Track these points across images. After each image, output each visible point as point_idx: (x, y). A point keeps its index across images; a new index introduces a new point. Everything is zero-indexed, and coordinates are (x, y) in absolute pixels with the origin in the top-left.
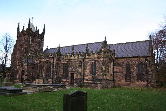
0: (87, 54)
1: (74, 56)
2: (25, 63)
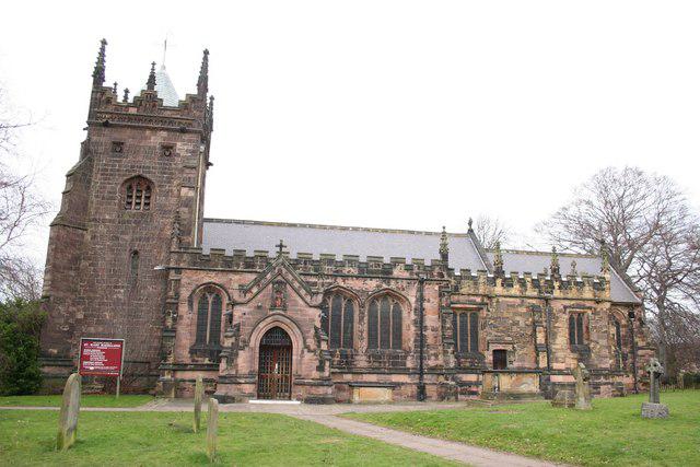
0: (556, 284)
1: (507, 283)
2: (303, 292)
